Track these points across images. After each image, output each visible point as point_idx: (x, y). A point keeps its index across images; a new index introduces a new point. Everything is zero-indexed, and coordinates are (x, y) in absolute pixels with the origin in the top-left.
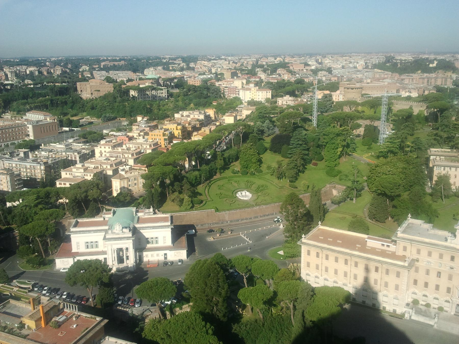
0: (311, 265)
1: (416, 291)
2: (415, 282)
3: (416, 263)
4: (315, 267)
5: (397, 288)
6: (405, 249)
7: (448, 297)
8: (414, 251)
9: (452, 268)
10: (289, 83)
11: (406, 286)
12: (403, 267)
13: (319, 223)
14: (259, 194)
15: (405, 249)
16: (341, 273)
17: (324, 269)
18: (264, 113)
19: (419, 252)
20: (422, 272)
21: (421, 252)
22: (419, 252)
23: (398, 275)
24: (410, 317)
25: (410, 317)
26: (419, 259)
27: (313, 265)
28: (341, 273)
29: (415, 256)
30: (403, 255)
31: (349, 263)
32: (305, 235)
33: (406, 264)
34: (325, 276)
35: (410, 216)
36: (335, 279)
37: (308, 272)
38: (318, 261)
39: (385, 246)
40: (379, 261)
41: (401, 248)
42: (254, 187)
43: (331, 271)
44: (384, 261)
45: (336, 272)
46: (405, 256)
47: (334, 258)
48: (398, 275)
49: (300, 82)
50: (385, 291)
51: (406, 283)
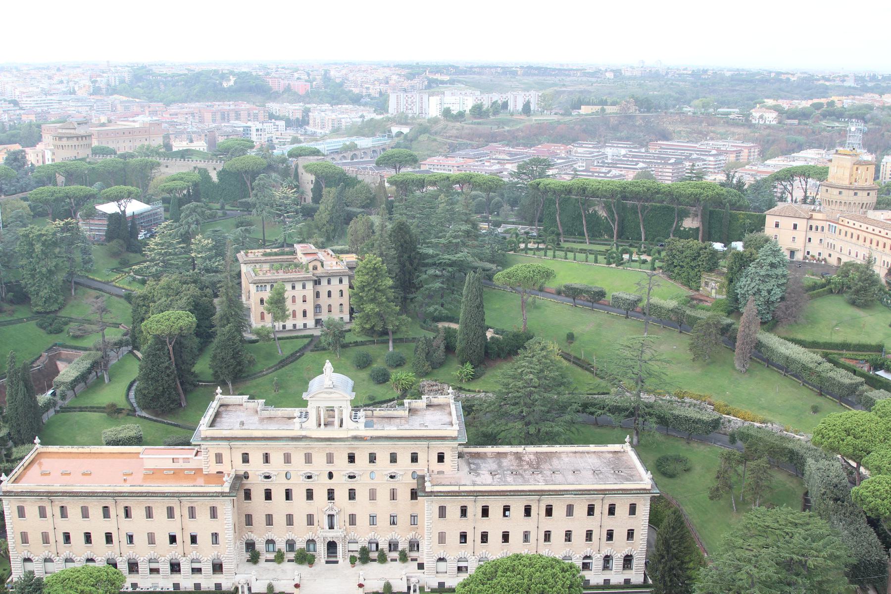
0: (30, 537)
1: (253, 537)
2: (249, 520)
3: (245, 481)
4: (41, 539)
6: (219, 458)
7: (311, 533)
9: (309, 477)
11: (233, 532)
12: (222, 494)
13: (35, 441)
15: (219, 458)
16: (98, 538)
17: (61, 539)
19: (246, 459)
20: (258, 495)
21: (251, 458)
22: (246, 459)
23: (214, 513)
24: (249, 589)
25: (249, 589)
26: (249, 472)
27: (35, 538)
28: (98, 538)
29: (242, 468)
30: (218, 473)
31: (112, 512)
32: (7, 475)
33: (227, 490)
35: (219, 390)
36: (88, 554)
38: (46, 525)
39: (181, 461)
40: (173, 495)
41: (213, 458)
44: (182, 493)
45: (88, 538)
46: (222, 473)
47: (80, 510)
48: (214, 513)
50: (194, 552)
51: (232, 527)
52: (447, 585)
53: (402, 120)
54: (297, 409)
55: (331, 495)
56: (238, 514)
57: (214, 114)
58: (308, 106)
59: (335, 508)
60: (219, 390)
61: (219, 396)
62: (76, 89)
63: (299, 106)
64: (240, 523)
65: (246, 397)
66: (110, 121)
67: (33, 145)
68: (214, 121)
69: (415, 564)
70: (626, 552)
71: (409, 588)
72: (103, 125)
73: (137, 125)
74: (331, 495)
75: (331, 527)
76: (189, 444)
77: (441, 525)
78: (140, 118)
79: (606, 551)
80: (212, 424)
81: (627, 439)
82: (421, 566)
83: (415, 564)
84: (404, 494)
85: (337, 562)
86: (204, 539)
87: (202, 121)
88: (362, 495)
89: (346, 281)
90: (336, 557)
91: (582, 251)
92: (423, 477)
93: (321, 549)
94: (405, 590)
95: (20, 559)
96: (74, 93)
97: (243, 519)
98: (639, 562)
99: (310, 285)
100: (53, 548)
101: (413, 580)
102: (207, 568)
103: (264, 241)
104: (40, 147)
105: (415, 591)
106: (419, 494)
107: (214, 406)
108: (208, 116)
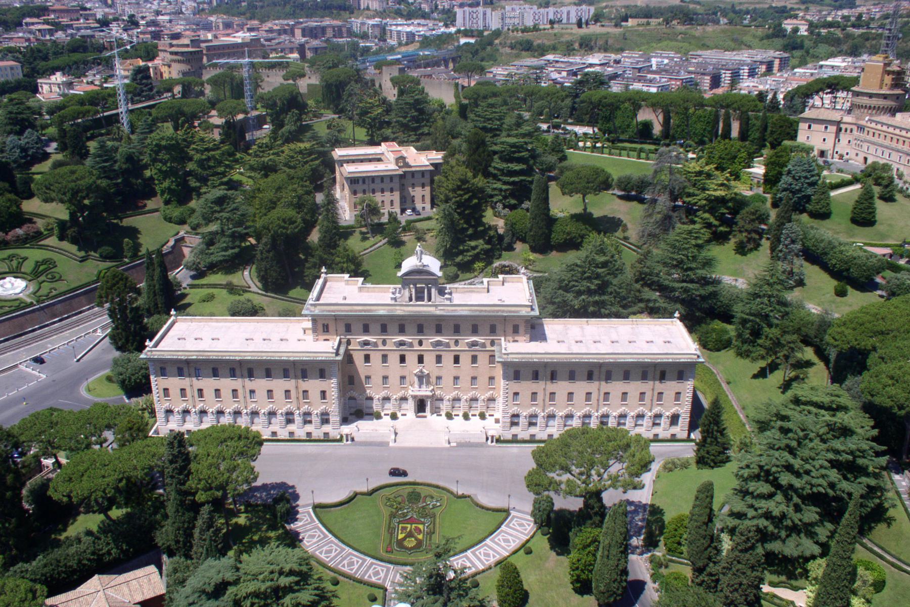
1: (355, 394)
5: (323, 394)
8: (342, 328)
10: (58, 49)
14: (43, 278)
18: (16, 113)
34: (200, 406)
37: (166, 405)
41: (320, 328)
42: (28, 267)
43: (209, 394)
49: (80, 46)
52: (519, 437)
53: (467, 33)
54: (392, 286)
55: (421, 360)
56: (343, 375)
57: (303, 30)
58: (384, 21)
59: (424, 370)
60: (324, 270)
61: (323, 275)
62: (184, 10)
63: (376, 21)
64: (343, 382)
65: (346, 276)
66: (216, 37)
67: (152, 59)
68: (304, 36)
69: (492, 419)
70: (673, 410)
71: (487, 439)
72: (211, 41)
73: (240, 41)
74: (421, 360)
75: (421, 384)
76: (301, 315)
77: (515, 386)
78: (240, 34)
79: (656, 410)
80: (318, 299)
81: (677, 315)
82: (497, 421)
83: (492, 419)
84: (483, 358)
85: (425, 417)
86: (314, 395)
87: (293, 35)
88: (448, 359)
89: (427, 176)
90: (424, 411)
91: (634, 150)
92: (500, 345)
93: (411, 405)
94: (485, 440)
95: (163, 410)
96: (181, 13)
97: (346, 379)
98: (684, 421)
99: (396, 180)
100: (190, 401)
101: (490, 433)
102: (315, 419)
103: (354, 140)
104: (158, 62)
105: (492, 442)
106: (497, 359)
107: (320, 282)
108: (298, 32)
